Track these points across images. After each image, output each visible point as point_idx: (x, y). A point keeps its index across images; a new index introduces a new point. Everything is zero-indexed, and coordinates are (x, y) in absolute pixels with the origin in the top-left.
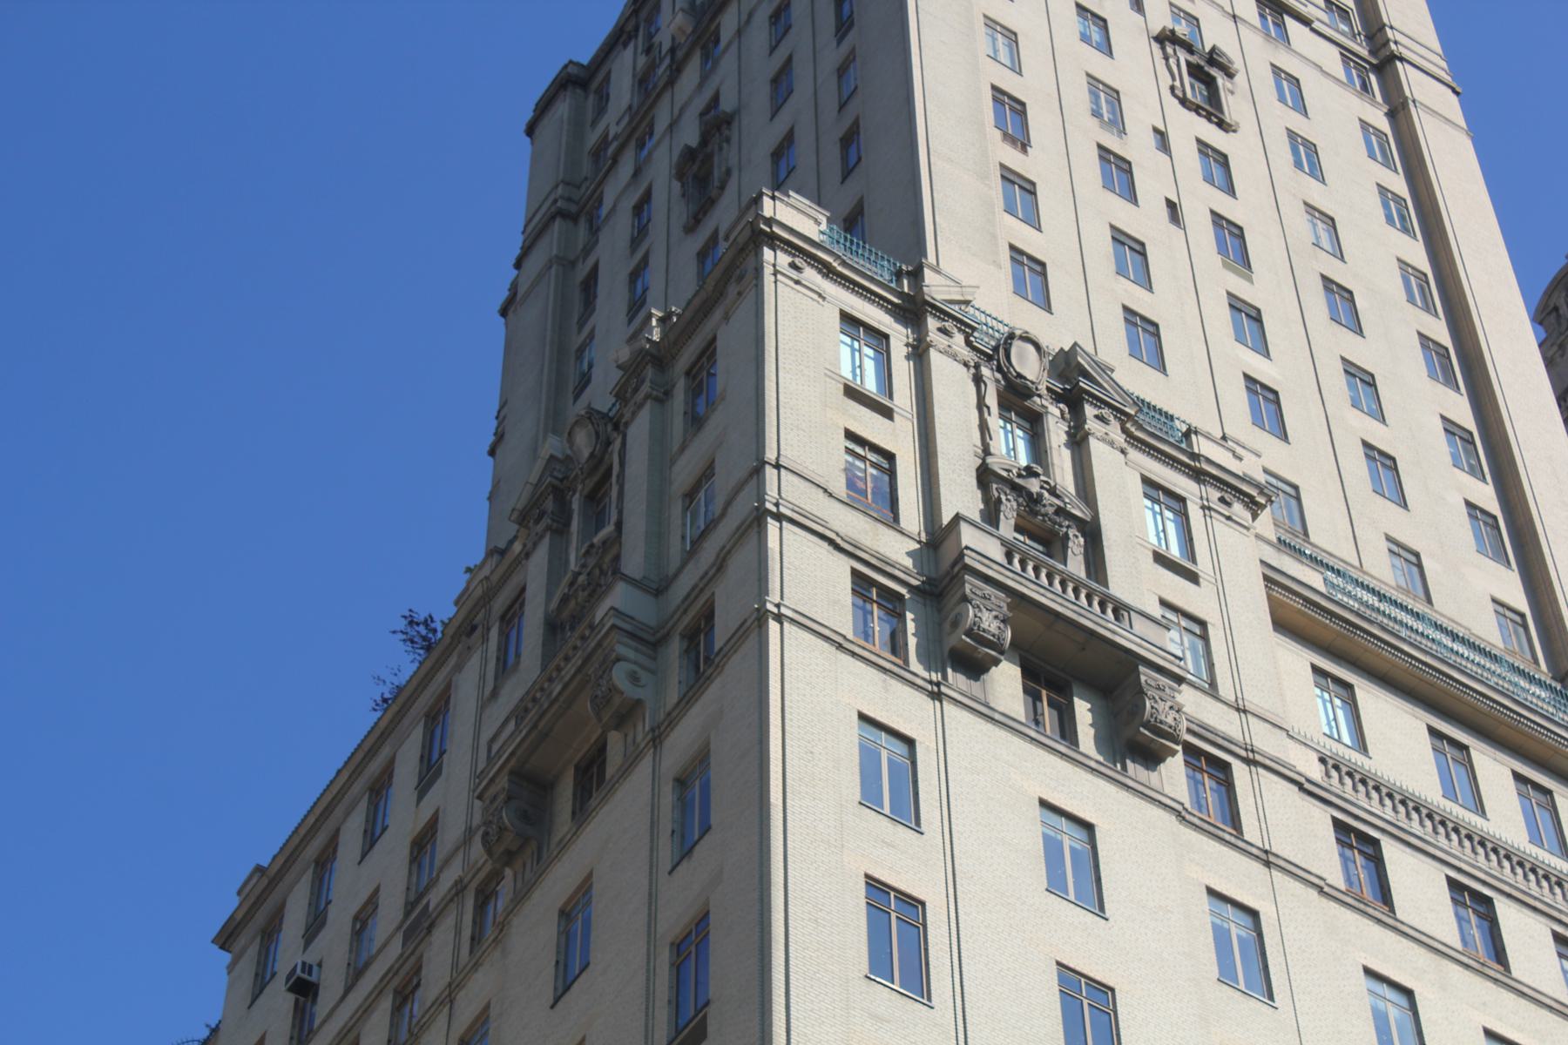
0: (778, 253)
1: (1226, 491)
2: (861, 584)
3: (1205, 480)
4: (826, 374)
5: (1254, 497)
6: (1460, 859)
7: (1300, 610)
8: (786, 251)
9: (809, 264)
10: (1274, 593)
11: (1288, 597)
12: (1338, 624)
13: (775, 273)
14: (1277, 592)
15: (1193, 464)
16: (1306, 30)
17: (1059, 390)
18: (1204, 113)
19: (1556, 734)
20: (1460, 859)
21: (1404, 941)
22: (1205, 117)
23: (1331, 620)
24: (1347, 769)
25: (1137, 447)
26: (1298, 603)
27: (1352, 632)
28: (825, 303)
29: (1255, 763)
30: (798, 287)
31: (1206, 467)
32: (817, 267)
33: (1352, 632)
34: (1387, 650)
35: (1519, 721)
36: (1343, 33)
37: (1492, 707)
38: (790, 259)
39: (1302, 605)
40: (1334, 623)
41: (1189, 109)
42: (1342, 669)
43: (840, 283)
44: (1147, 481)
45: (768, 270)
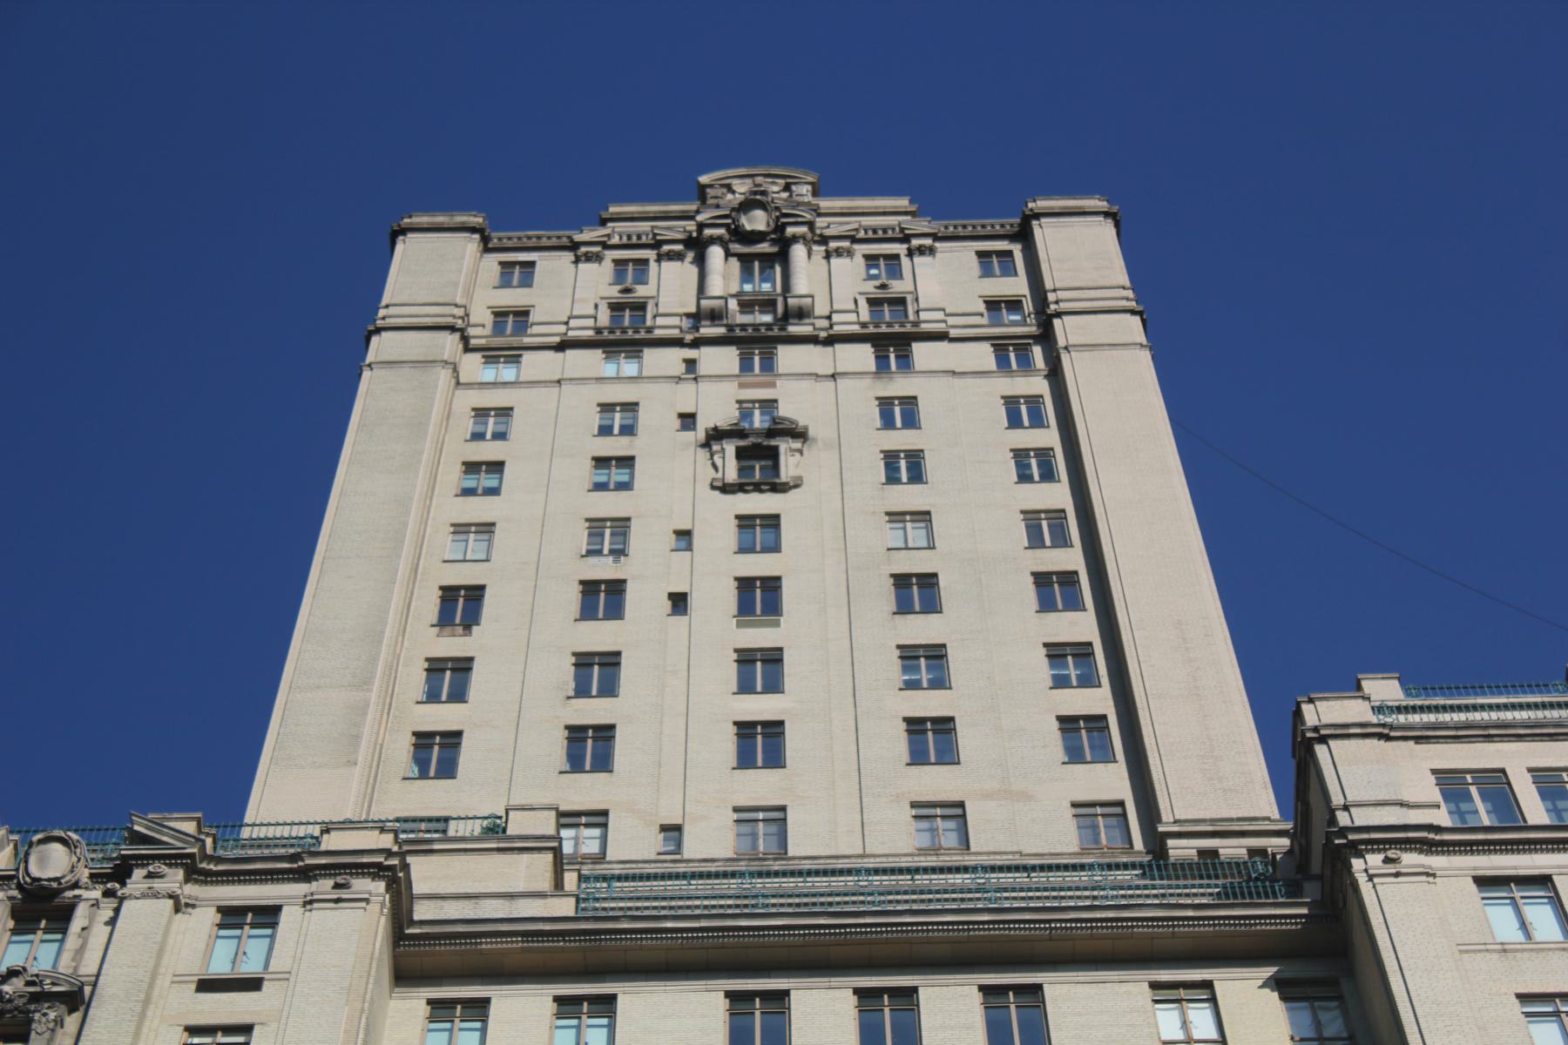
0: (1367, 856)
1: (335, 875)
3: (316, 875)
4: (1461, 952)
5: (381, 863)
7: (522, 948)
8: (1373, 851)
10: (484, 946)
11: (507, 942)
12: (575, 941)
13: (1371, 878)
14: (487, 943)
15: (295, 866)
16: (944, 345)
17: (109, 871)
18: (751, 488)
19: (1015, 922)
22: (754, 490)
23: (564, 941)
25: (357, 874)
26: (517, 942)
27: (595, 940)
28: (1437, 880)
30: (1400, 879)
31: (310, 861)
32: (1416, 849)
33: (595, 940)
34: (647, 939)
35: (846, 933)
36: (1014, 324)
37: (805, 935)
38: (331, 882)
39: (523, 942)
40: (570, 941)
41: (733, 492)
42: (444, 988)
43: (283, 879)
44: (1483, 882)
45: (1362, 879)
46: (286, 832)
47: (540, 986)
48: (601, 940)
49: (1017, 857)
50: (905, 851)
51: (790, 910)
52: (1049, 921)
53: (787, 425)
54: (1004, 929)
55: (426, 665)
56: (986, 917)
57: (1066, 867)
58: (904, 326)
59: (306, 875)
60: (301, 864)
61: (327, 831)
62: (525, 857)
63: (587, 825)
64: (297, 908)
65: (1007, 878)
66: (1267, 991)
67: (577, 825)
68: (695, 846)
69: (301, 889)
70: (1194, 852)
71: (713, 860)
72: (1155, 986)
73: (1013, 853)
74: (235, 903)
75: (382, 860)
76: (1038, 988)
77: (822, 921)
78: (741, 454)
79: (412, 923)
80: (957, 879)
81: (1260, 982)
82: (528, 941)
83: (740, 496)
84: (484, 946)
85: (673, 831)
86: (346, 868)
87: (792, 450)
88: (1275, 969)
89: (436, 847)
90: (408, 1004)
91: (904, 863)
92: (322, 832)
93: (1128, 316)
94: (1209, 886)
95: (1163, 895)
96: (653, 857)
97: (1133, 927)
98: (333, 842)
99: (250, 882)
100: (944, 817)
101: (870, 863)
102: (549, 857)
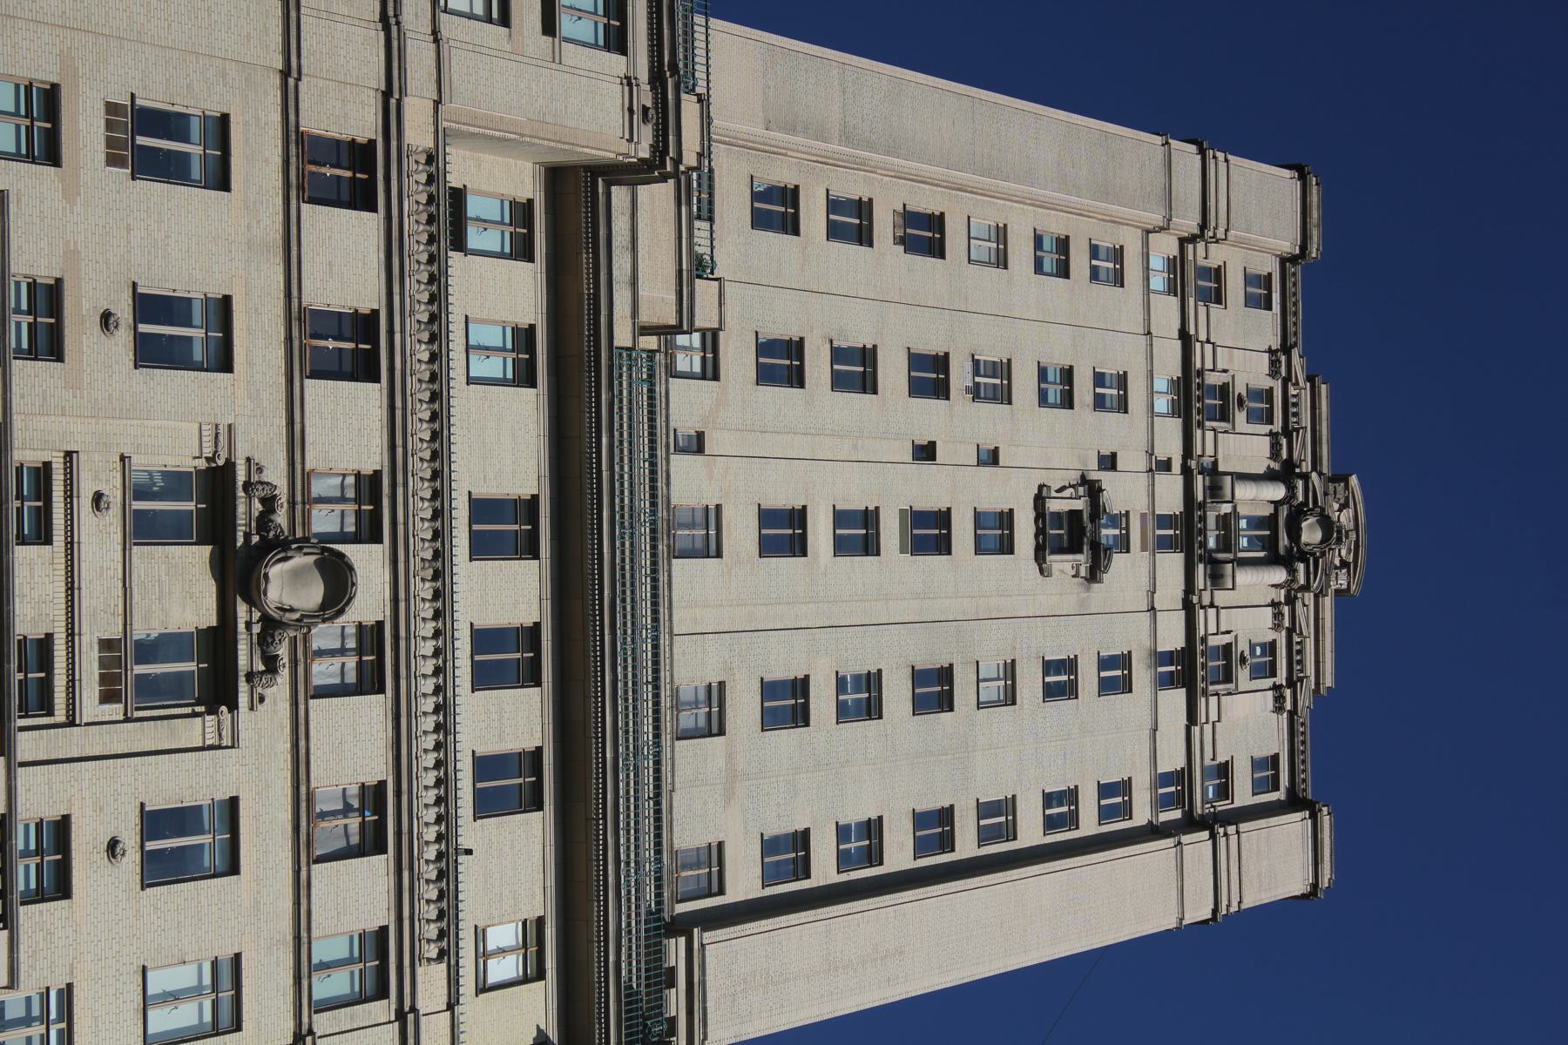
1: (656, 108)
2: (374, 796)
3: (657, 90)
6: (403, 331)
9: (657, 124)
10: (585, 256)
12: (589, 346)
14: (588, 259)
16: (1183, 721)
20: (403, 331)
21: (279, 200)
23: (589, 336)
24: (439, 449)
25: (657, 130)
26: (589, 289)
27: (590, 367)
29: (387, 29)
31: (669, 80)
33: (590, 367)
34: (591, 418)
36: (1204, 791)
37: (594, 574)
38: (649, 104)
39: (589, 295)
40: (589, 341)
41: (1036, 508)
42: (543, 216)
46: (700, 59)
47: (545, 311)
48: (590, 372)
49: (669, 787)
50: (675, 676)
51: (618, 561)
52: (605, 818)
53: (1103, 562)
54: (597, 774)
55: (865, 199)
56: (609, 755)
57: (658, 836)
58: (1203, 681)
59: (657, 79)
60: (668, 74)
61: (700, 101)
62: (673, 297)
63: (704, 359)
64: (625, 70)
65: (648, 776)
66: (535, 1034)
67: (704, 349)
68: (681, 465)
69: (643, 75)
70: (673, 963)
71: (668, 484)
72: (540, 922)
73: (673, 783)
74: (630, 9)
75: (671, 155)
76: (540, 807)
77: (606, 592)
78: (1074, 515)
79: (608, 185)
80: (648, 728)
81: (543, 1027)
82: (589, 299)
83: (1032, 515)
84: (585, 256)
85: (697, 444)
86: (663, 119)
87: (1078, 566)
88: (556, 1042)
89: (683, 209)
90: (528, 180)
91: (664, 675)
92: (699, 95)
93: (1212, 906)
94: (638, 978)
95: (630, 932)
96: (672, 425)
97: (599, 901)
98: (690, 107)
99: (650, 24)
100: (709, 714)
101: (664, 641)
102: (673, 322)
